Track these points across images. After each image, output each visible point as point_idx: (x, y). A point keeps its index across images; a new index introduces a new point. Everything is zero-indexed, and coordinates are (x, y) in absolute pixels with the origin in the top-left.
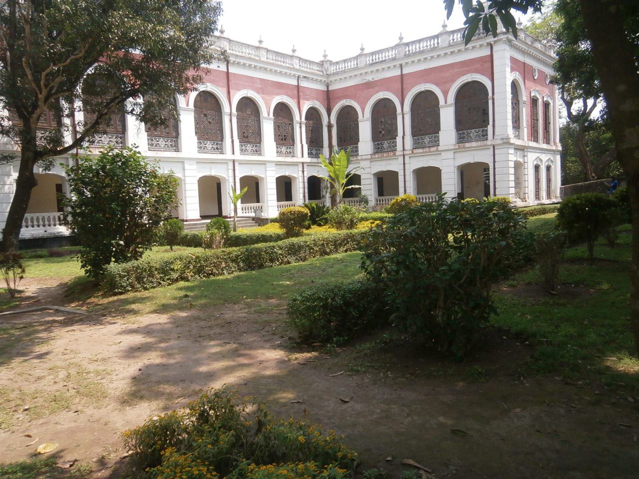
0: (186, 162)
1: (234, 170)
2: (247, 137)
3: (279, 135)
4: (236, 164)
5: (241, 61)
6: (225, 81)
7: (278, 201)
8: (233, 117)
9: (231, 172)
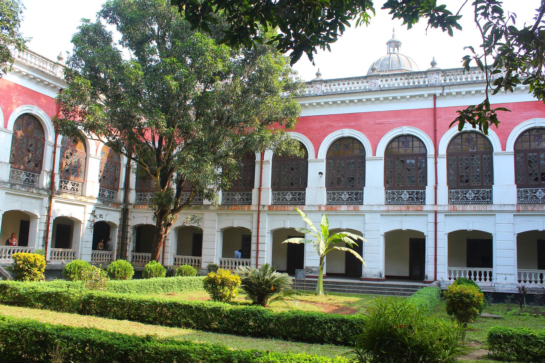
0: (366, 215)
1: (436, 224)
2: (467, 181)
3: (531, 174)
4: (440, 217)
5: (451, 91)
6: (432, 119)
7: (519, 267)
8: (438, 160)
9: (432, 227)
